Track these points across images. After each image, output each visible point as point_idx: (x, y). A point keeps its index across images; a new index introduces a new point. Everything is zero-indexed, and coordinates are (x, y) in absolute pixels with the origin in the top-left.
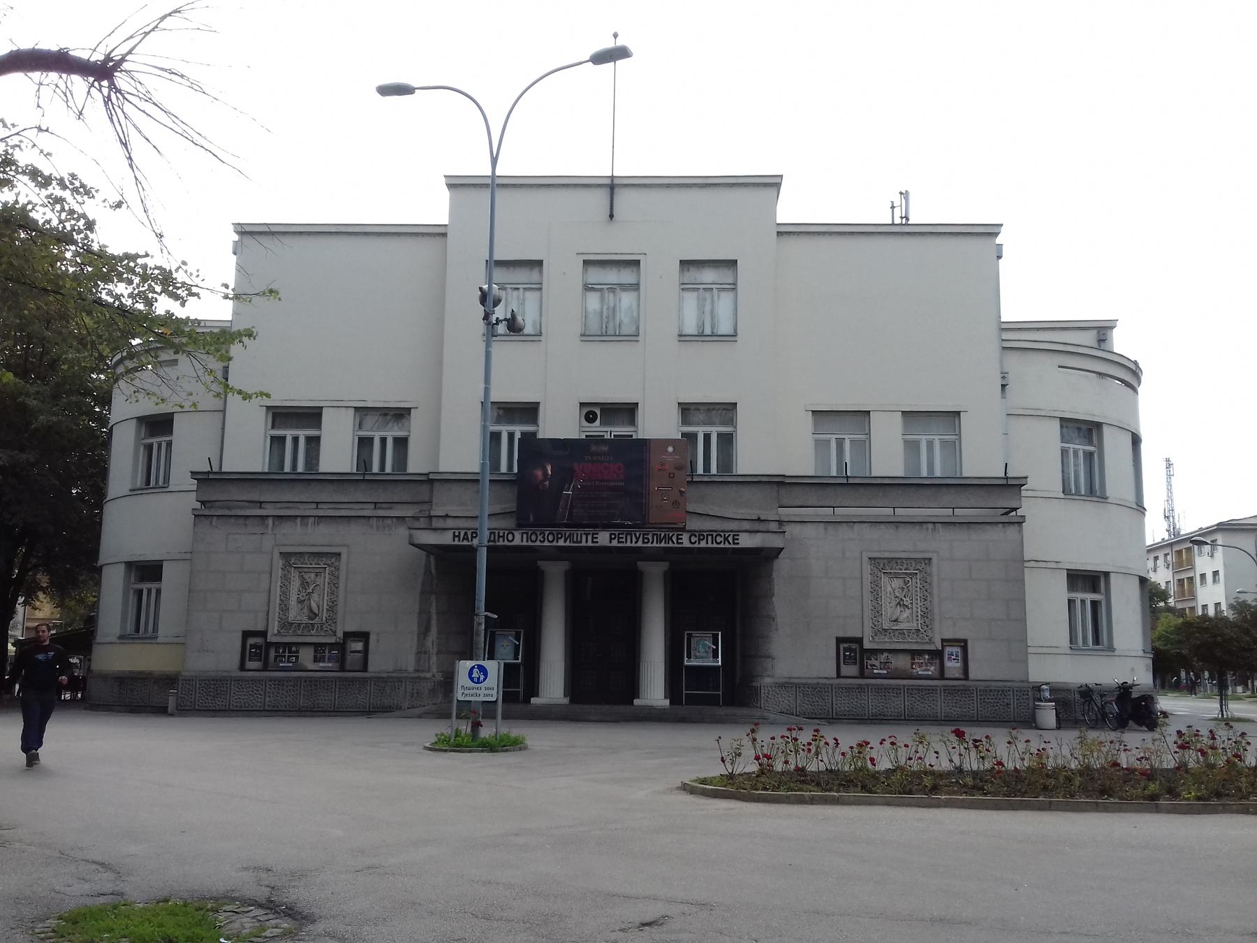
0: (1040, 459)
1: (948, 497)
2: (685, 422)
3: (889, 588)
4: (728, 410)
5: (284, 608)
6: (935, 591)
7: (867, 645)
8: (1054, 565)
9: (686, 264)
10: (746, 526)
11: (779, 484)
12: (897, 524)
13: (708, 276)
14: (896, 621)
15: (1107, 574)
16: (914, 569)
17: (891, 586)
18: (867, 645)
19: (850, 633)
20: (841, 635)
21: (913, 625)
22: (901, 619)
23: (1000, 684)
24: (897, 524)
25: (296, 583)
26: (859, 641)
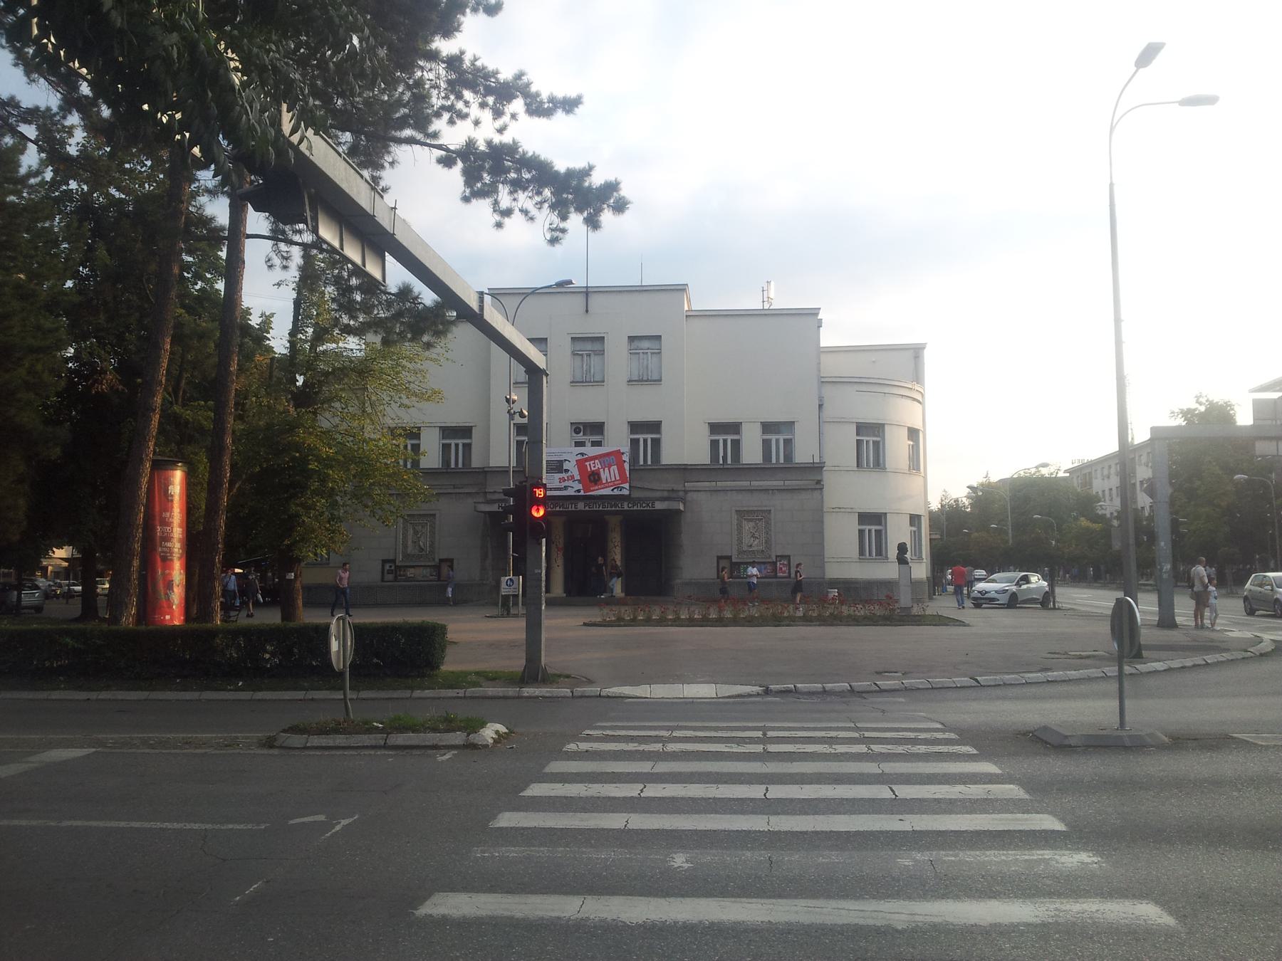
2: (632, 432)
4: (655, 427)
5: (405, 546)
9: (632, 339)
10: (658, 494)
11: (685, 470)
12: (751, 491)
13: (646, 344)
16: (762, 516)
17: (748, 526)
24: (751, 491)
25: (411, 532)
26: (729, 558)
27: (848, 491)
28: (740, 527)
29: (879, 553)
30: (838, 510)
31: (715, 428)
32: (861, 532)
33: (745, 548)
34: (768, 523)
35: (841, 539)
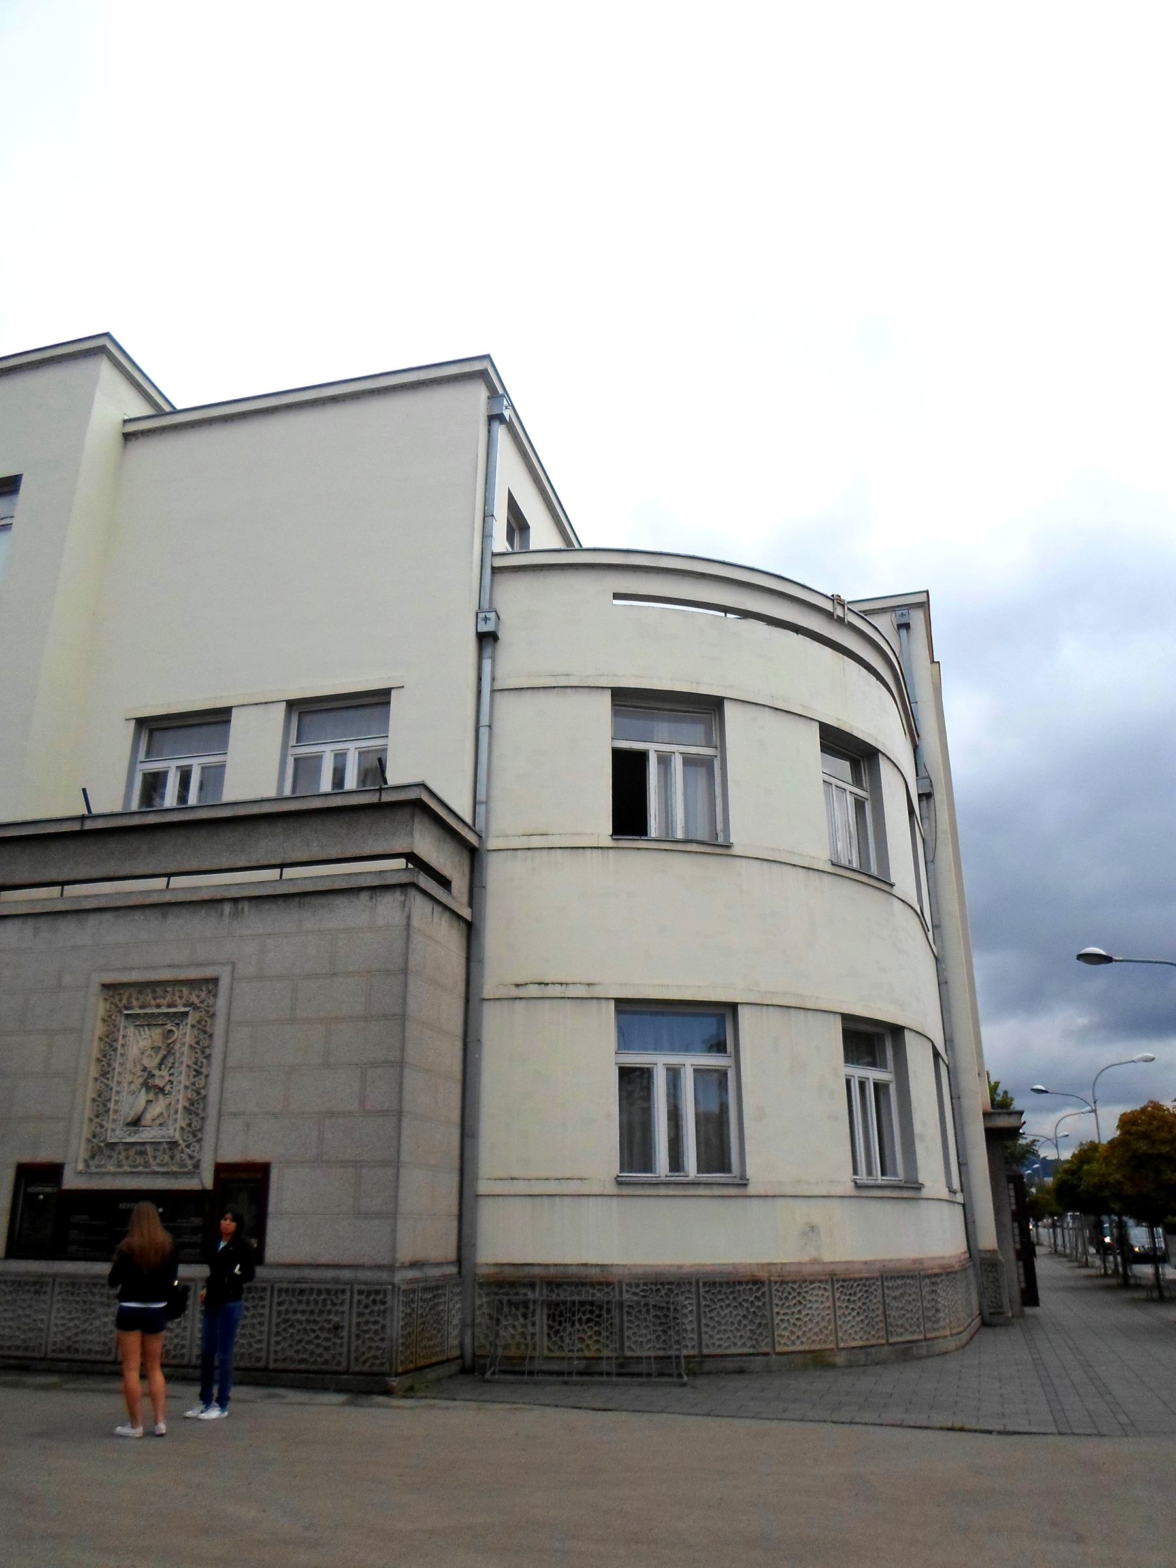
0: (556, 774)
1: (268, 845)
3: (133, 1052)
6: (217, 1052)
7: (71, 1181)
8: (581, 992)
14: (136, 1123)
15: (733, 1007)
17: (138, 1044)
18: (71, 1181)
19: (44, 1155)
20: (27, 1157)
21: (172, 1132)
22: (148, 1117)
23: (329, 1274)
26: (54, 1171)
27: (585, 921)
28: (110, 1042)
29: (718, 1151)
30: (535, 994)
31: (154, 728)
32: (634, 1082)
33: (118, 1134)
34: (204, 1032)
35: (554, 1098)
